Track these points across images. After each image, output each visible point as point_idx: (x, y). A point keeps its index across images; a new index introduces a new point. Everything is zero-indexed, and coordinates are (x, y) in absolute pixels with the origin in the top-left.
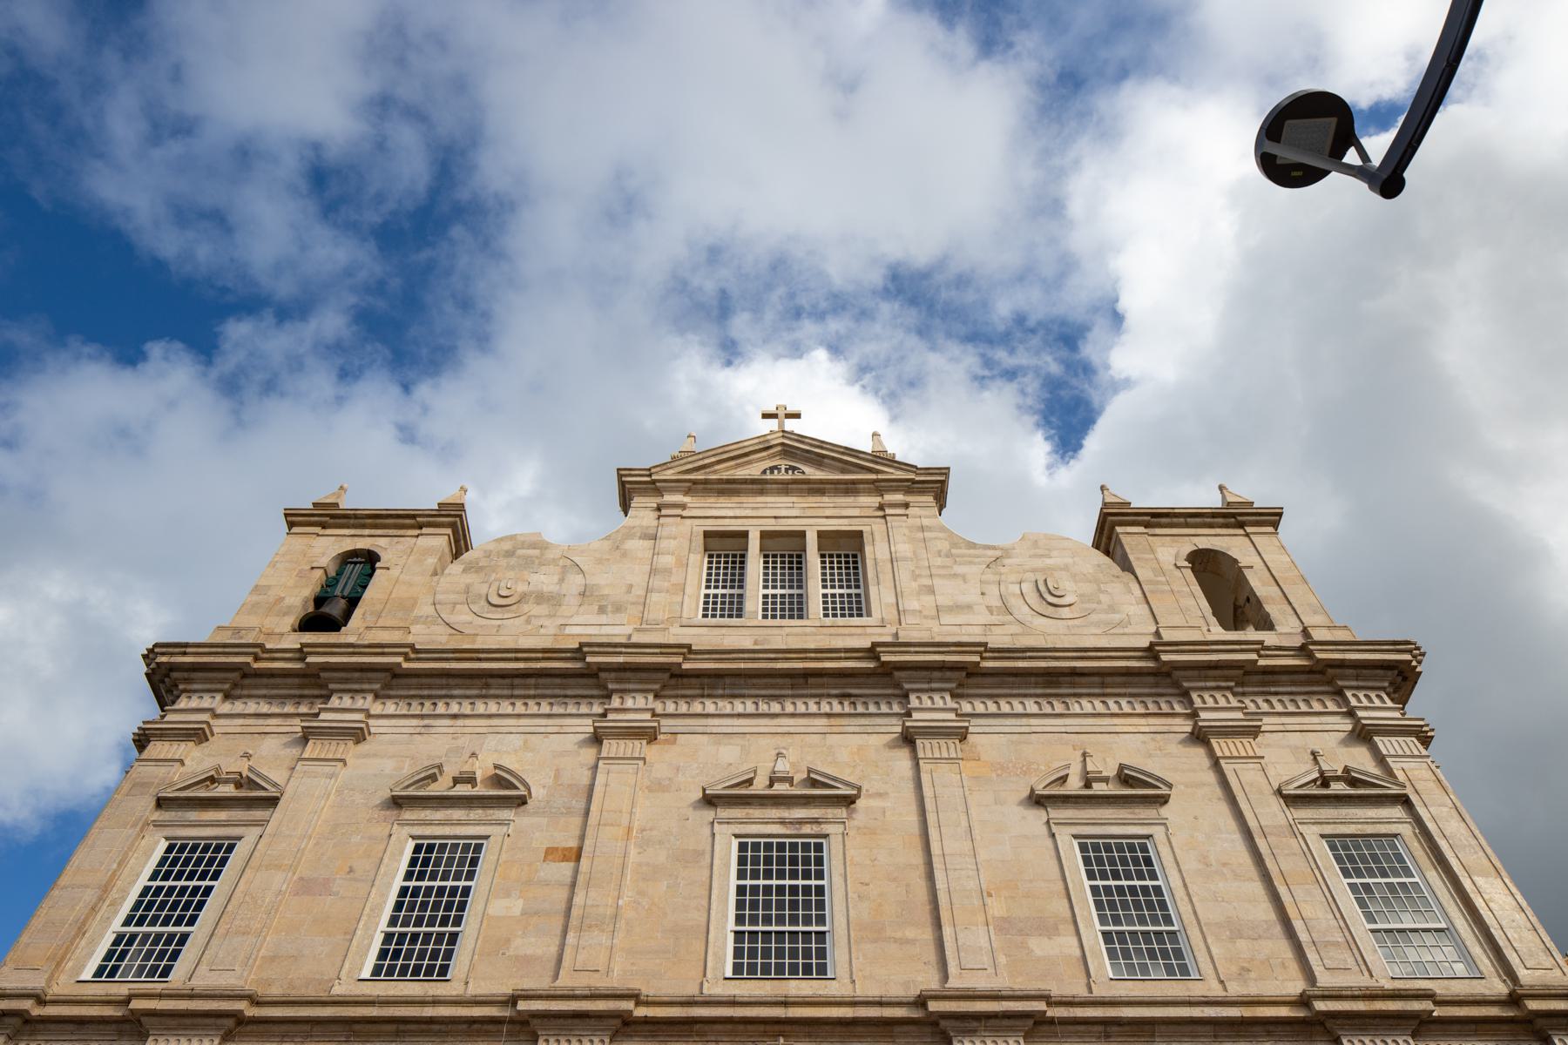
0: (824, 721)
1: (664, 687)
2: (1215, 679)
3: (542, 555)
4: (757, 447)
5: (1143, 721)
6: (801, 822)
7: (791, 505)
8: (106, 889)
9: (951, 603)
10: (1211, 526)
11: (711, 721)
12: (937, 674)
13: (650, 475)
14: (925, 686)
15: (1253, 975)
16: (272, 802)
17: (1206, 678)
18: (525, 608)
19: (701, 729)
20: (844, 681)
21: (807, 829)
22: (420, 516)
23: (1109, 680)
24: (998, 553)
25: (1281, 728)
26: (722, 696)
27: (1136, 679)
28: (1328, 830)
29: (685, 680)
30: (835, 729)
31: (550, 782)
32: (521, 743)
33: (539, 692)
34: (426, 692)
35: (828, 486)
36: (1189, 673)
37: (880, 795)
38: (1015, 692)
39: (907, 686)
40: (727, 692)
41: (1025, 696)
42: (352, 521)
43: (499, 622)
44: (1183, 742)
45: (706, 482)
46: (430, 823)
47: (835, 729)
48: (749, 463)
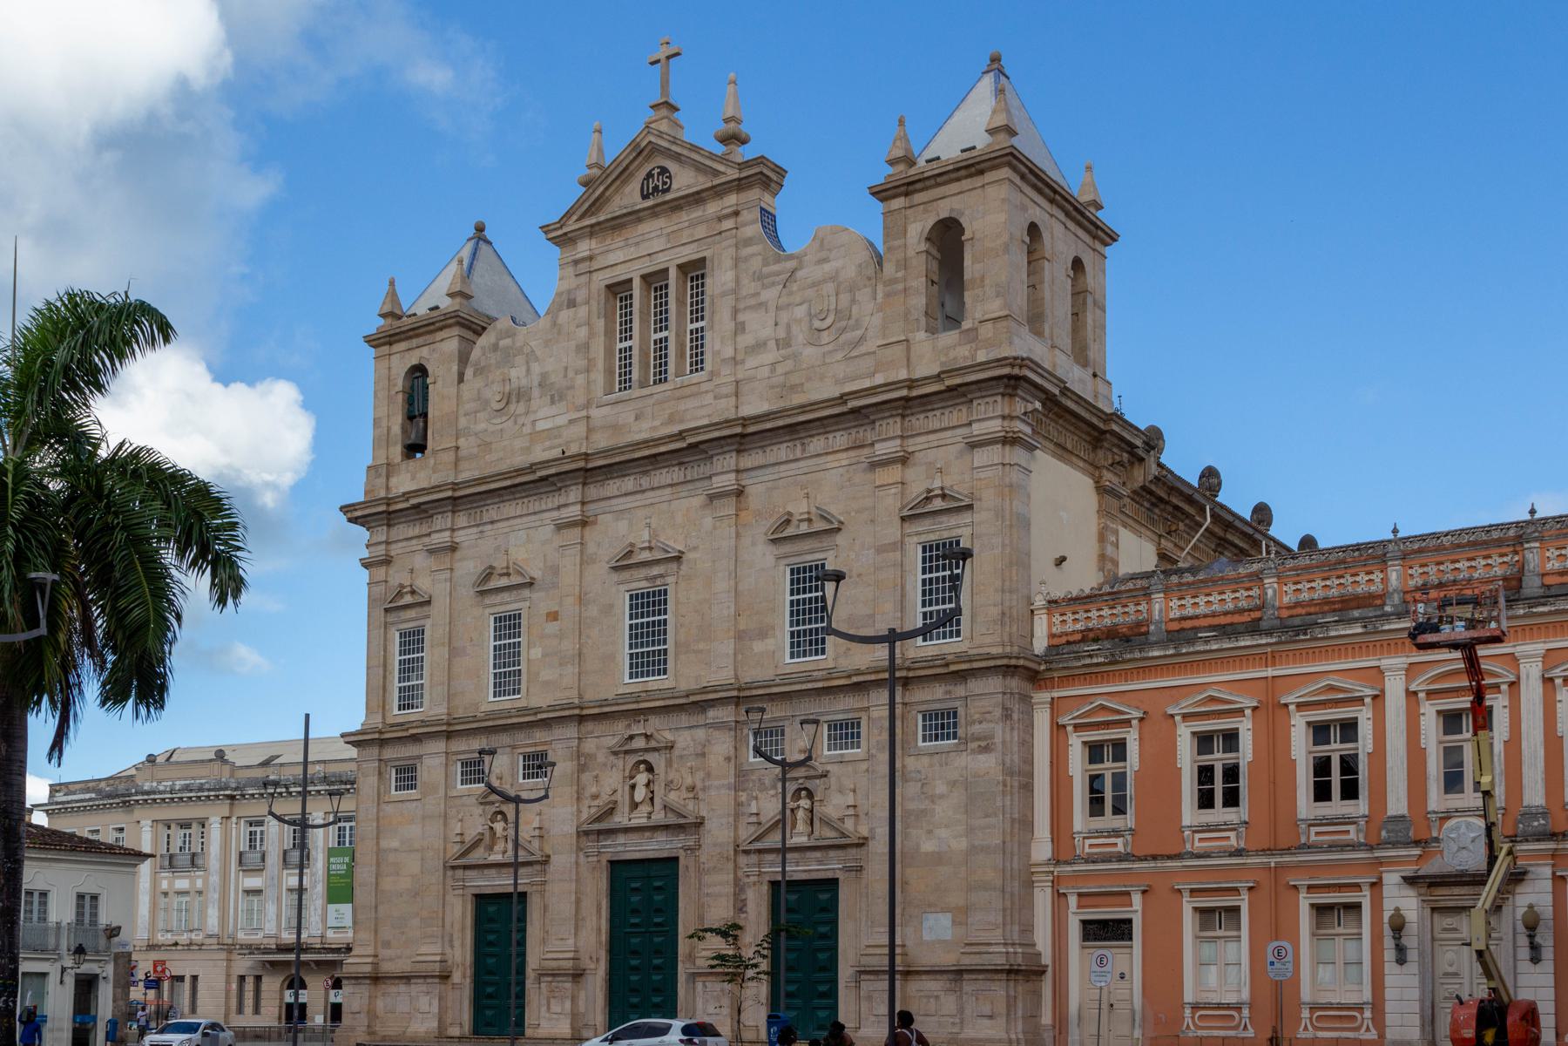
0: (668, 491)
1: (586, 478)
2: (888, 409)
3: (513, 343)
4: (631, 157)
5: (844, 455)
6: (655, 577)
7: (659, 233)
8: (385, 666)
9: (753, 342)
10: (958, 180)
11: (614, 502)
12: (723, 442)
13: (561, 227)
14: (720, 451)
15: (851, 653)
16: (428, 603)
17: (882, 411)
18: (512, 407)
19: (607, 509)
20: (676, 455)
21: (658, 583)
22: (437, 322)
23: (825, 422)
24: (791, 264)
25: (926, 446)
26: (617, 477)
27: (842, 418)
28: (924, 538)
29: (594, 472)
30: (675, 496)
31: (541, 565)
32: (525, 536)
33: (527, 493)
34: (475, 505)
35: (682, 201)
36: (871, 409)
37: (695, 548)
38: (774, 441)
39: (710, 453)
40: (620, 474)
41: (781, 443)
42: (403, 336)
43: (500, 427)
44: (864, 470)
45: (599, 223)
46: (495, 605)
47: (675, 496)
48: (632, 175)
